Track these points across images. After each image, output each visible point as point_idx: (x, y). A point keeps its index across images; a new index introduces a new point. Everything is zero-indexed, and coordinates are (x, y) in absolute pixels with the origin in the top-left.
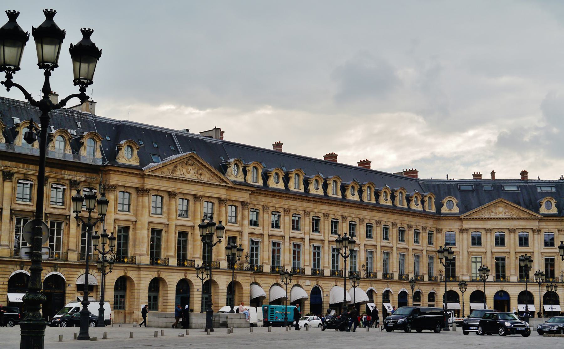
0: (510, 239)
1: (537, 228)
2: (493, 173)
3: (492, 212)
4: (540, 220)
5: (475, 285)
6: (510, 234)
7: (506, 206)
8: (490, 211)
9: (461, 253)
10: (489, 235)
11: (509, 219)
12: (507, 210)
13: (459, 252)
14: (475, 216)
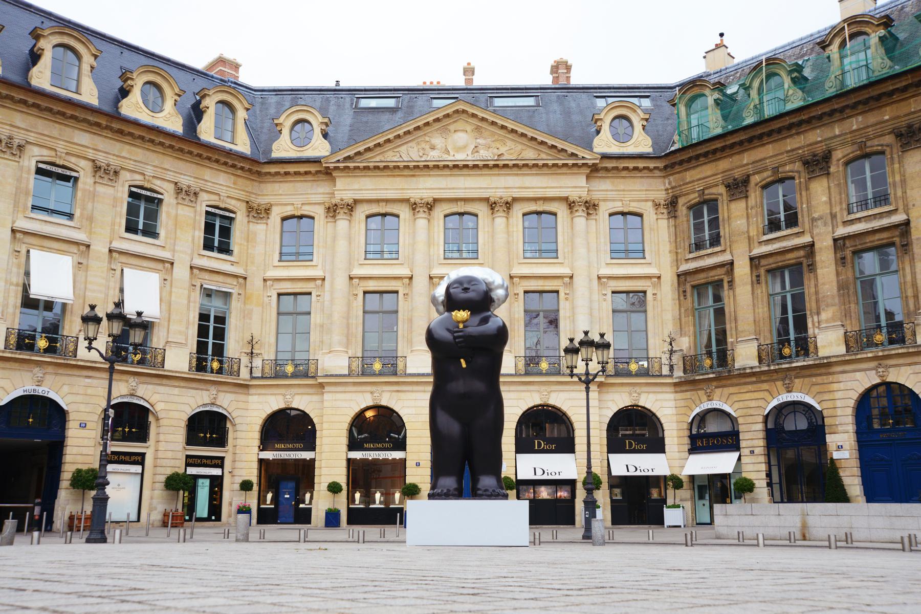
0: (493, 235)
1: (584, 194)
2: (469, 71)
3: (433, 148)
4: (594, 171)
5: (369, 388)
6: (493, 219)
7: (478, 128)
8: (427, 147)
9: (327, 282)
10: (422, 223)
11: (486, 166)
12: (481, 141)
13: (324, 279)
14: (377, 158)
